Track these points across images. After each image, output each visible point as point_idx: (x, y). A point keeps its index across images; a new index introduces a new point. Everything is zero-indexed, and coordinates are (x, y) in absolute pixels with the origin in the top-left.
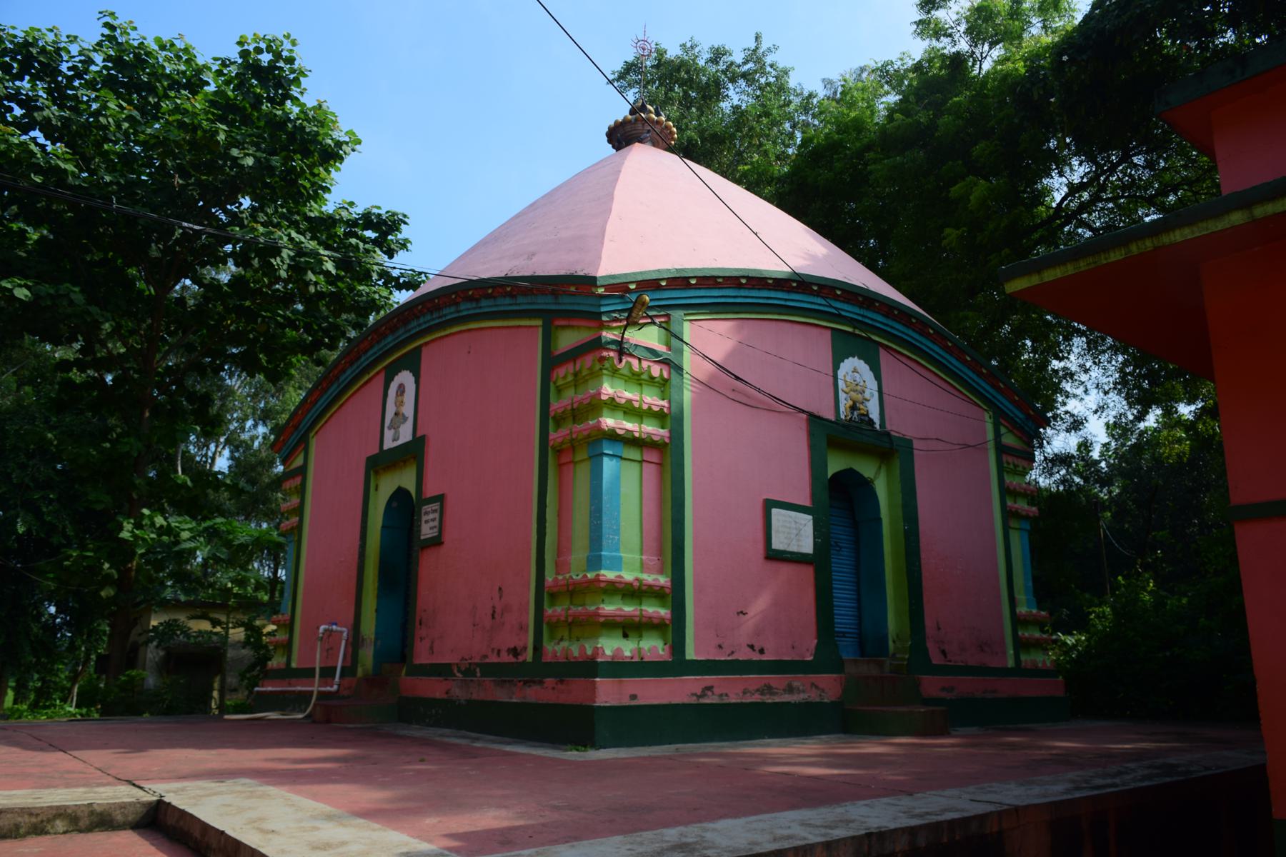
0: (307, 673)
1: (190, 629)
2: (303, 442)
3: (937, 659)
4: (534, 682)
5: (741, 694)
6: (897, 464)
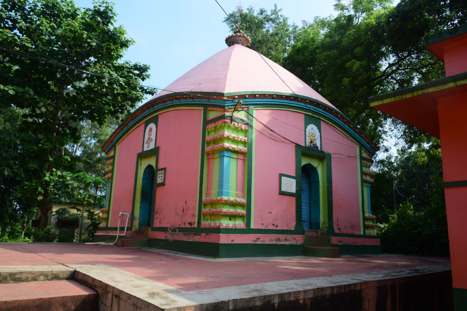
0: (115, 229)
1: (70, 212)
2: (114, 147)
3: (337, 231)
4: (198, 234)
6: (325, 162)
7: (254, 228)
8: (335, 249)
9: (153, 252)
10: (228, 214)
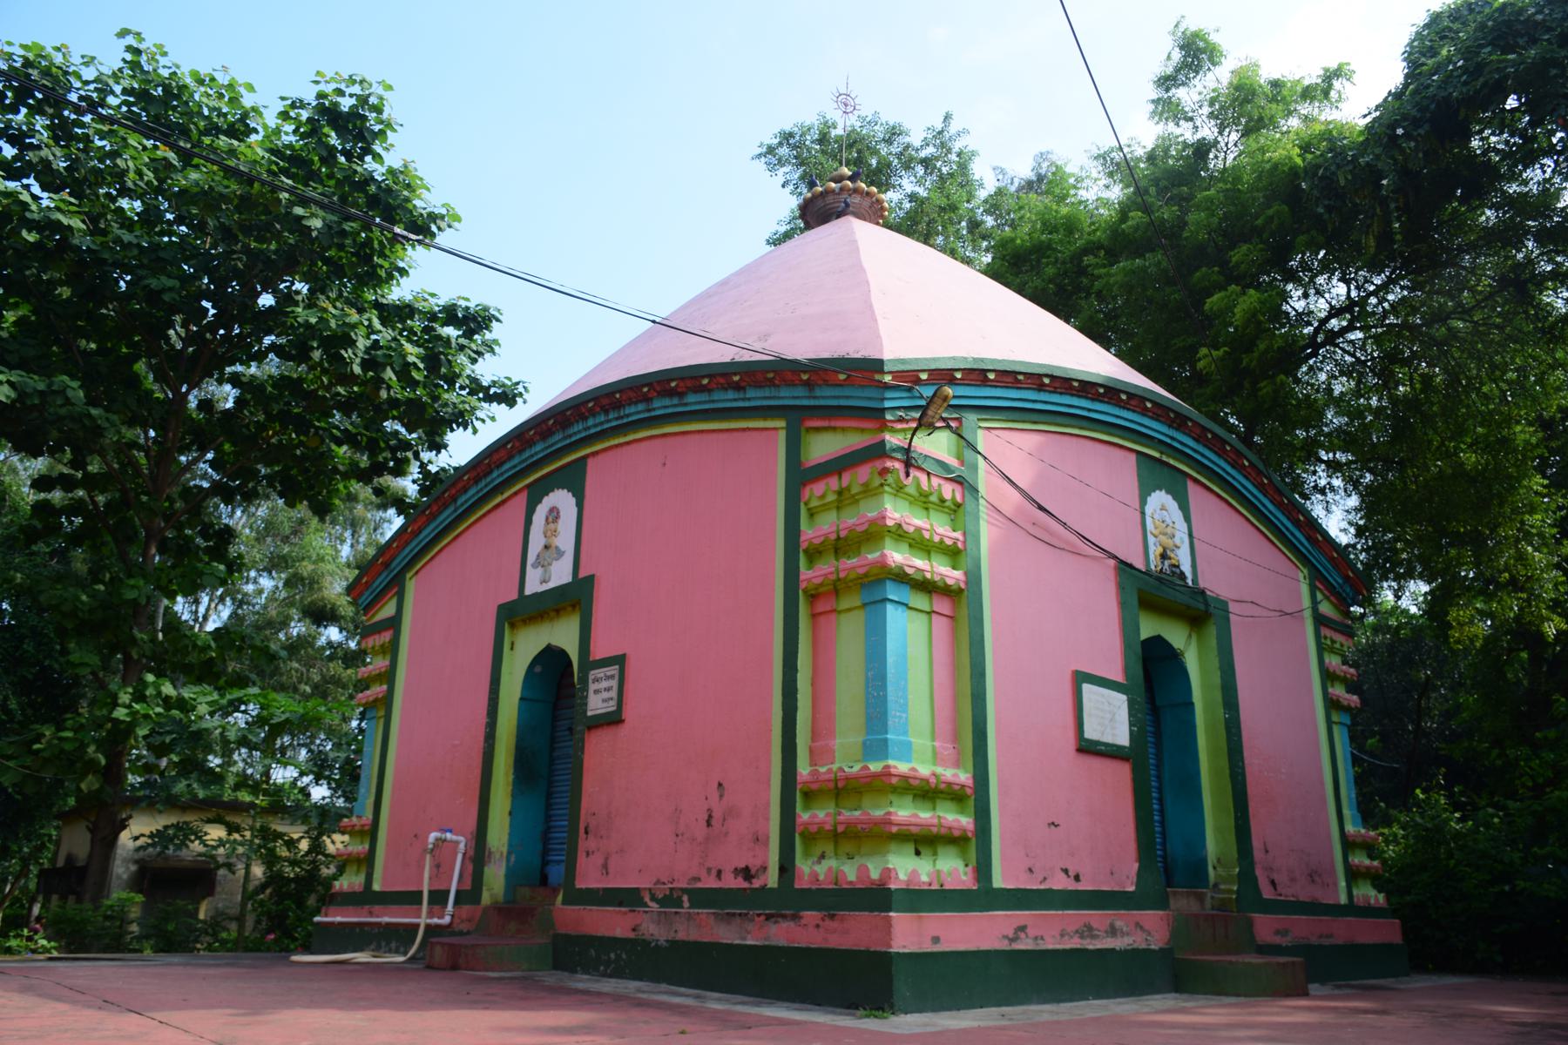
0: (413, 898)
1: (206, 834)
3: (1267, 893)
4: (784, 917)
5: (1059, 937)
6: (1212, 631)
7: (1003, 886)
8: (1293, 963)
9: (599, 994)
10: (914, 829)
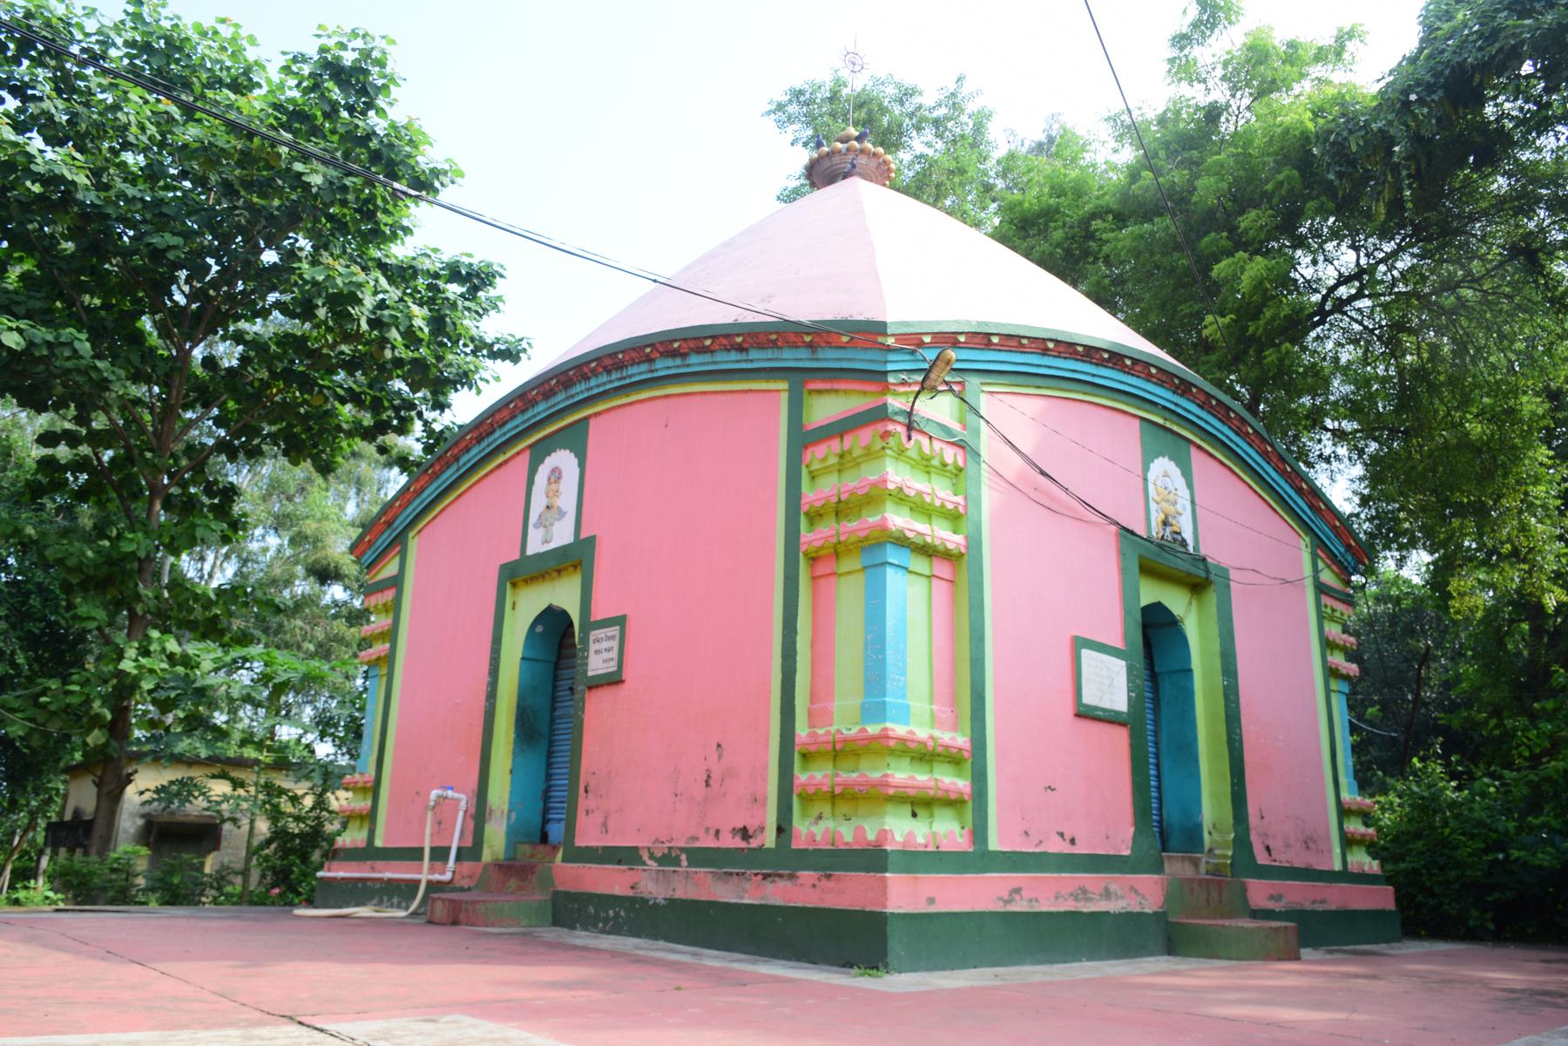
0: (414, 854)
1: (210, 790)
2: (400, 541)
3: (1262, 858)
4: (781, 876)
6: (1212, 598)
7: (999, 849)
8: (1286, 928)
9: (598, 950)
10: (911, 792)
